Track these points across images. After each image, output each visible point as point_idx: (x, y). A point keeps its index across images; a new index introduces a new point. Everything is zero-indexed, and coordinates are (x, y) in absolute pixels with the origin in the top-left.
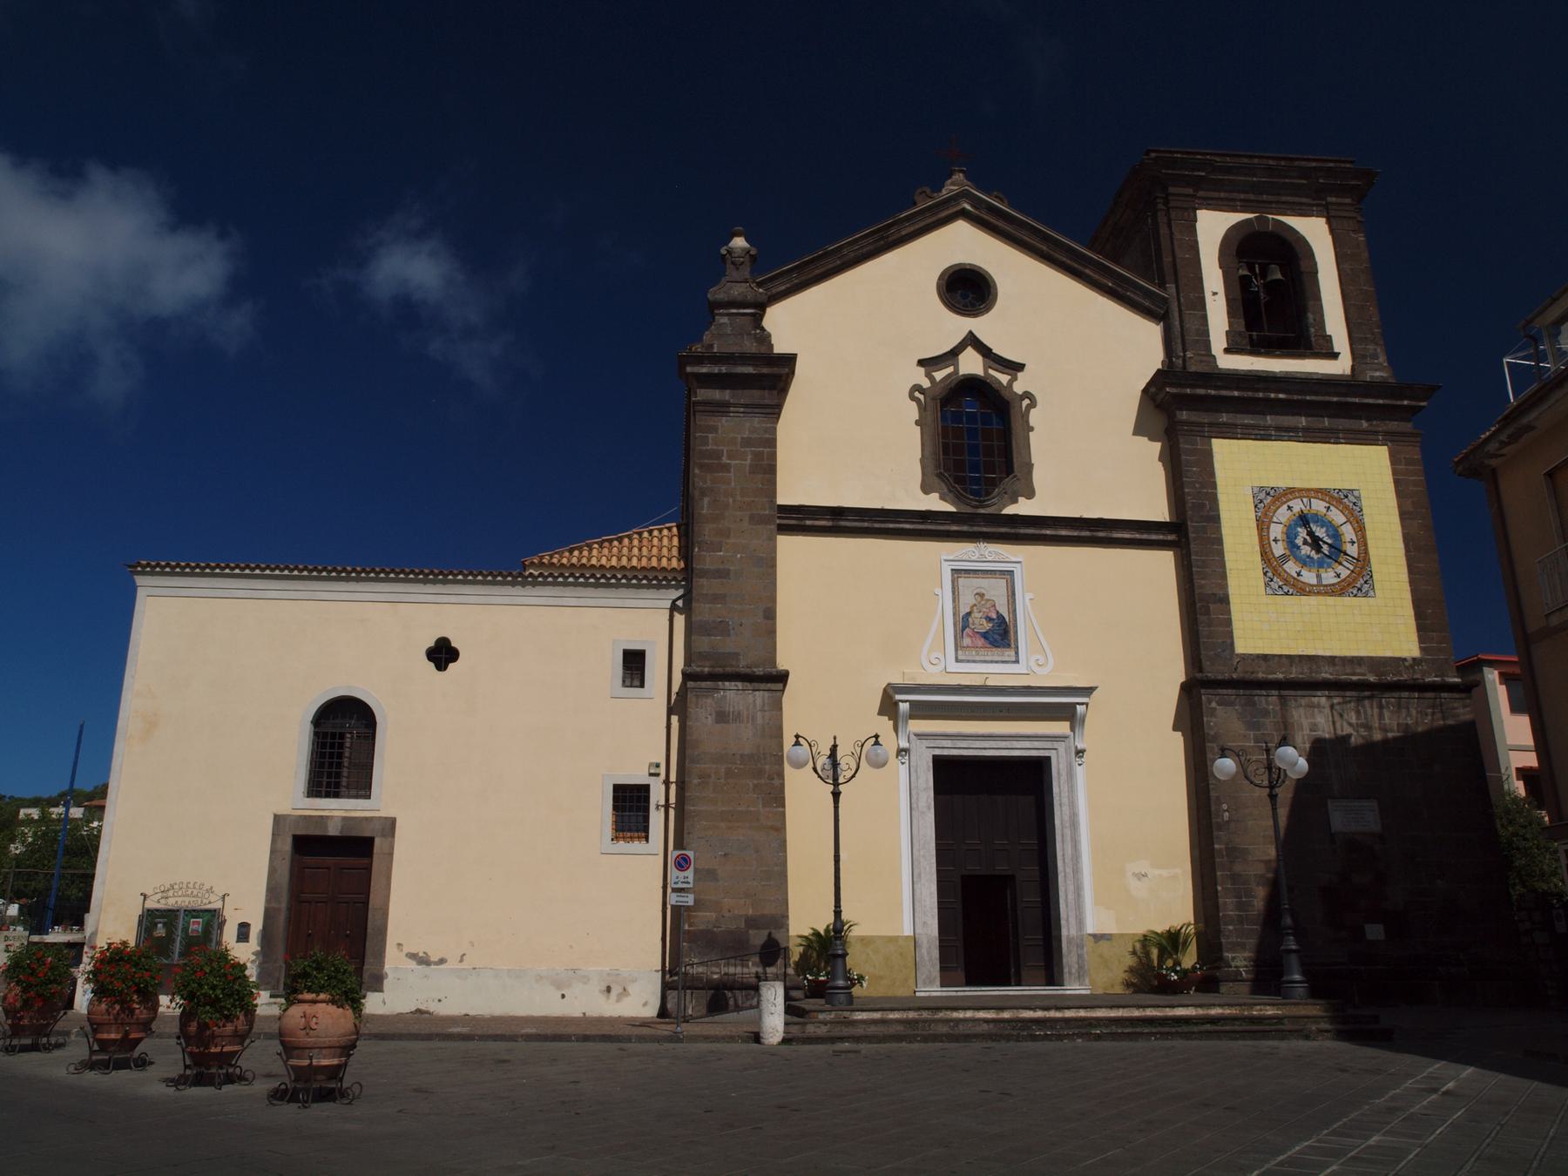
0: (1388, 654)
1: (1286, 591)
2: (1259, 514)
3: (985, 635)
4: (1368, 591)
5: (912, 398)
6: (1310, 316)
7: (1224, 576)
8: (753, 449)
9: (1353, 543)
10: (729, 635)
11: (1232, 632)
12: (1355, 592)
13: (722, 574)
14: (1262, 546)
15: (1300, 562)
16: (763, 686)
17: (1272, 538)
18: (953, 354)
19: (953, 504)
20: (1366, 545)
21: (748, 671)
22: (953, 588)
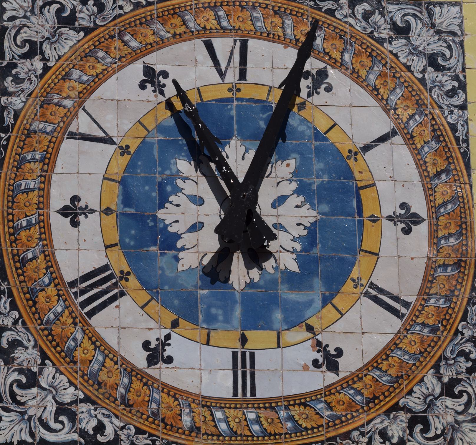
1: (89, 426)
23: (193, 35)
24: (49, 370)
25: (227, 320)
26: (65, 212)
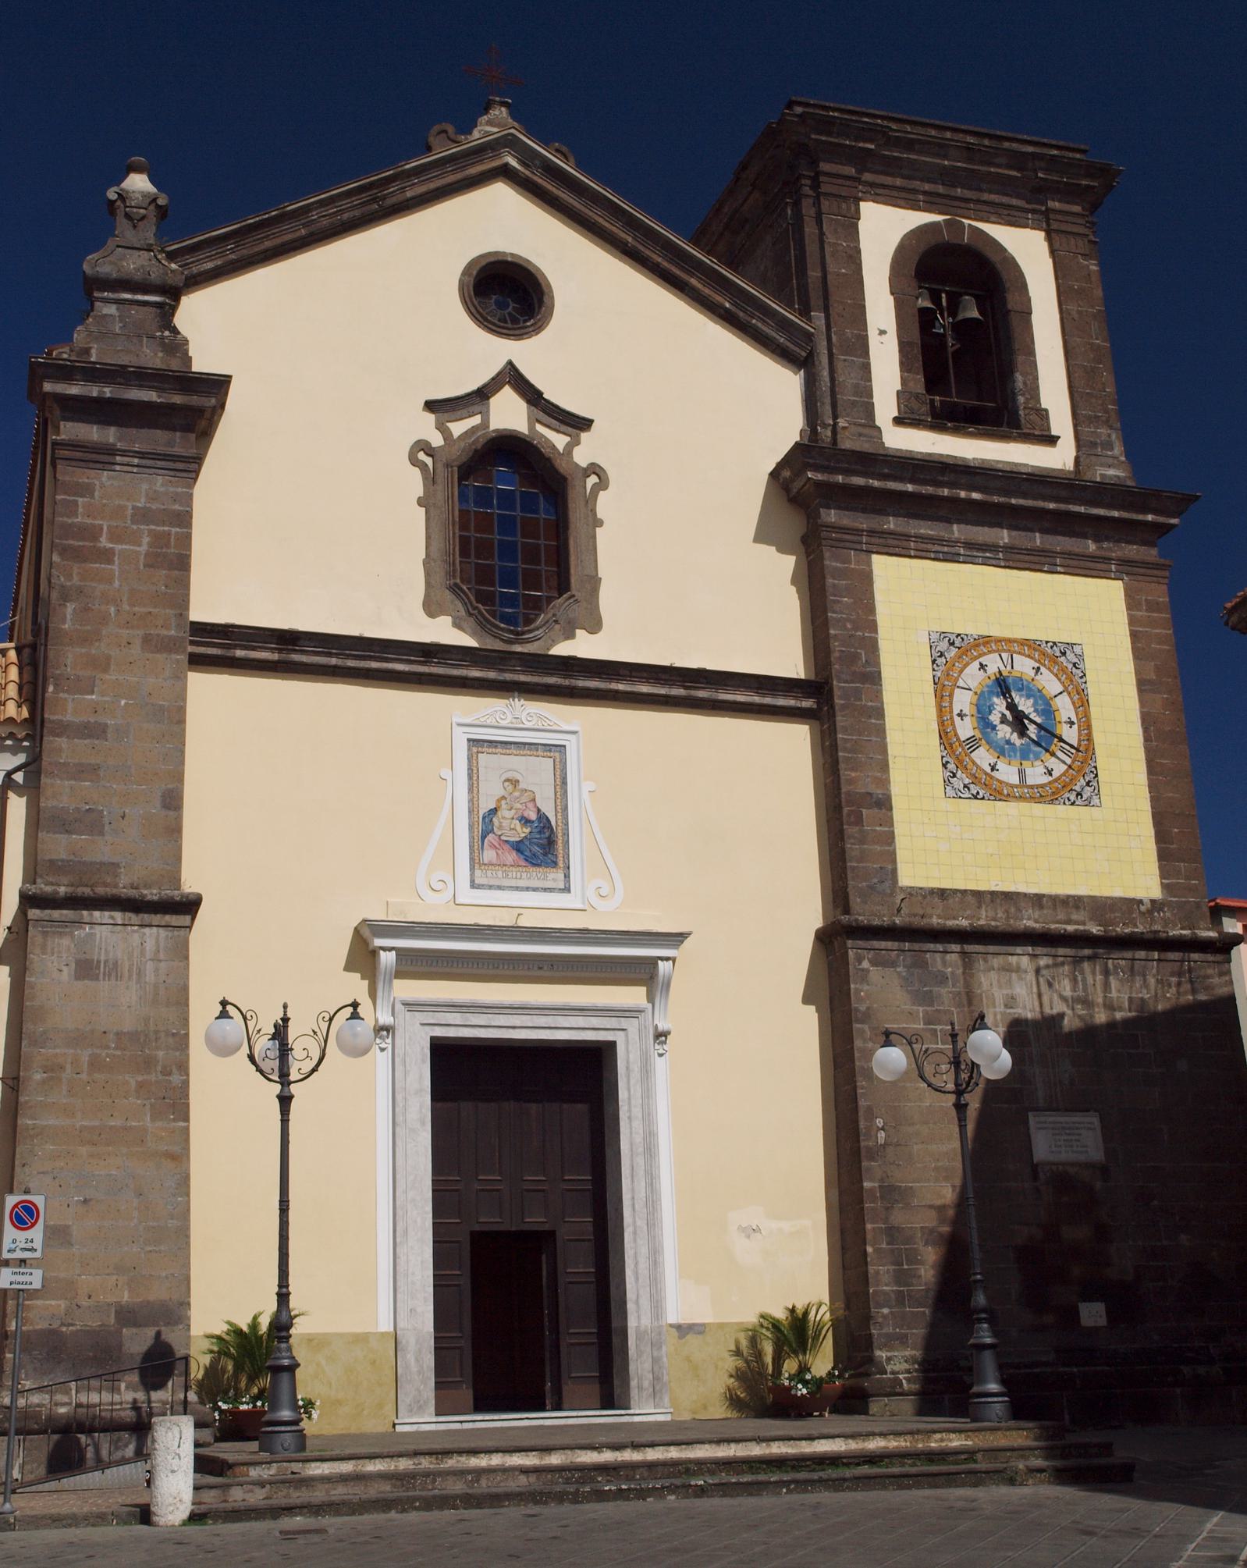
0: (1118, 893)
1: (975, 793)
2: (939, 674)
3: (518, 847)
4: (1091, 797)
5: (414, 461)
6: (1019, 378)
7: (885, 767)
8: (153, 527)
9: (1072, 723)
10: (101, 833)
11: (894, 853)
12: (1073, 797)
13: (94, 731)
14: (941, 723)
15: (995, 750)
16: (157, 919)
17: (956, 711)
18: (483, 394)
19: (473, 635)
20: (1089, 727)
21: (132, 893)
22: (470, 769)
23: (995, 651)
24: (959, 772)
25: (1015, 756)
26: (959, 715)
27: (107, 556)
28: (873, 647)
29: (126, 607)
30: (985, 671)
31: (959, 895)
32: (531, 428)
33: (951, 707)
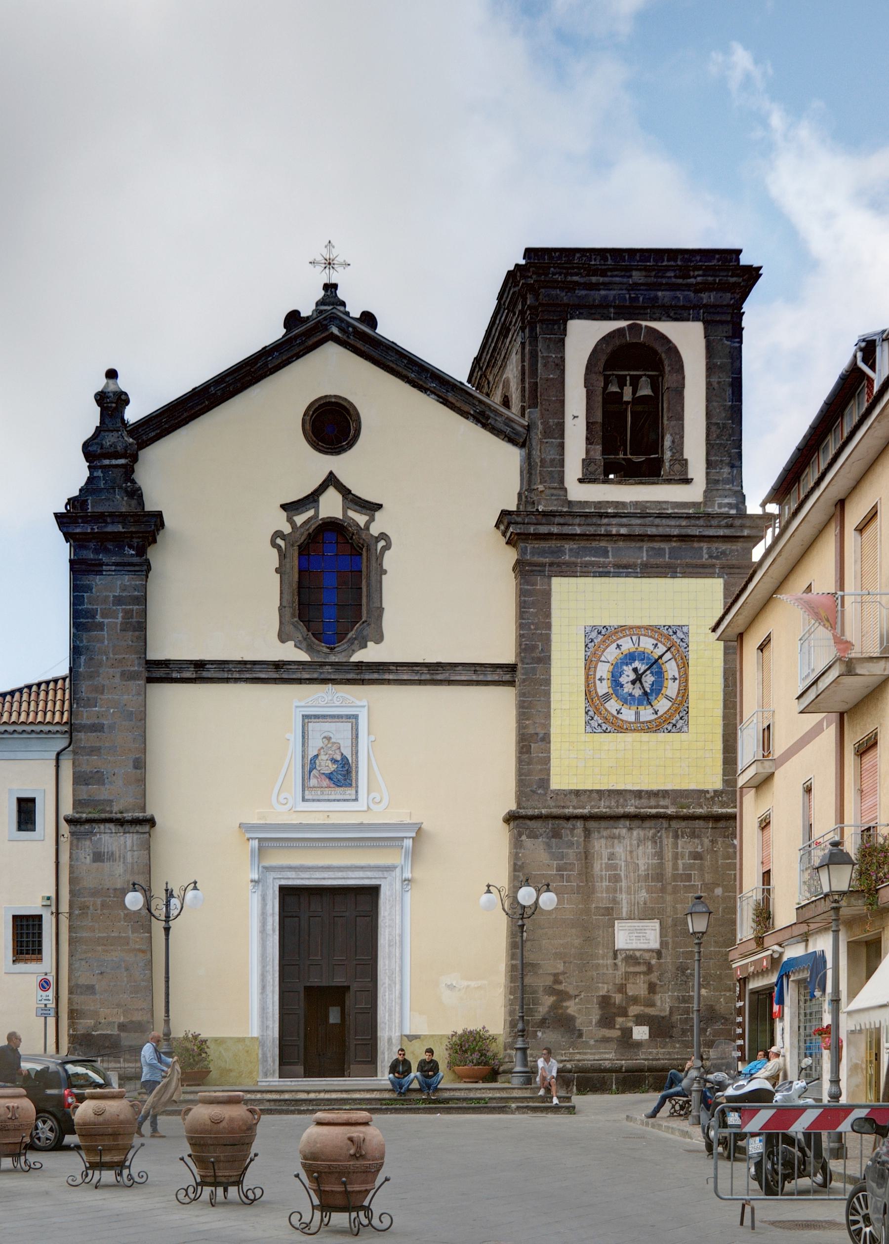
0: (693, 786)
1: (605, 728)
2: (589, 654)
3: (330, 777)
4: (682, 727)
5: (274, 544)
7: (548, 716)
8: (124, 607)
10: (104, 784)
11: (549, 769)
12: (669, 728)
13: (97, 728)
14: (587, 685)
15: (621, 701)
16: (133, 829)
17: (598, 677)
18: (312, 499)
20: (687, 681)
21: (119, 816)
22: (303, 732)
23: (627, 636)
24: (596, 716)
25: (634, 702)
26: (599, 679)
27: (100, 627)
28: (547, 640)
29: (111, 656)
30: (620, 649)
31: (588, 793)
32: (345, 513)
33: (595, 675)
